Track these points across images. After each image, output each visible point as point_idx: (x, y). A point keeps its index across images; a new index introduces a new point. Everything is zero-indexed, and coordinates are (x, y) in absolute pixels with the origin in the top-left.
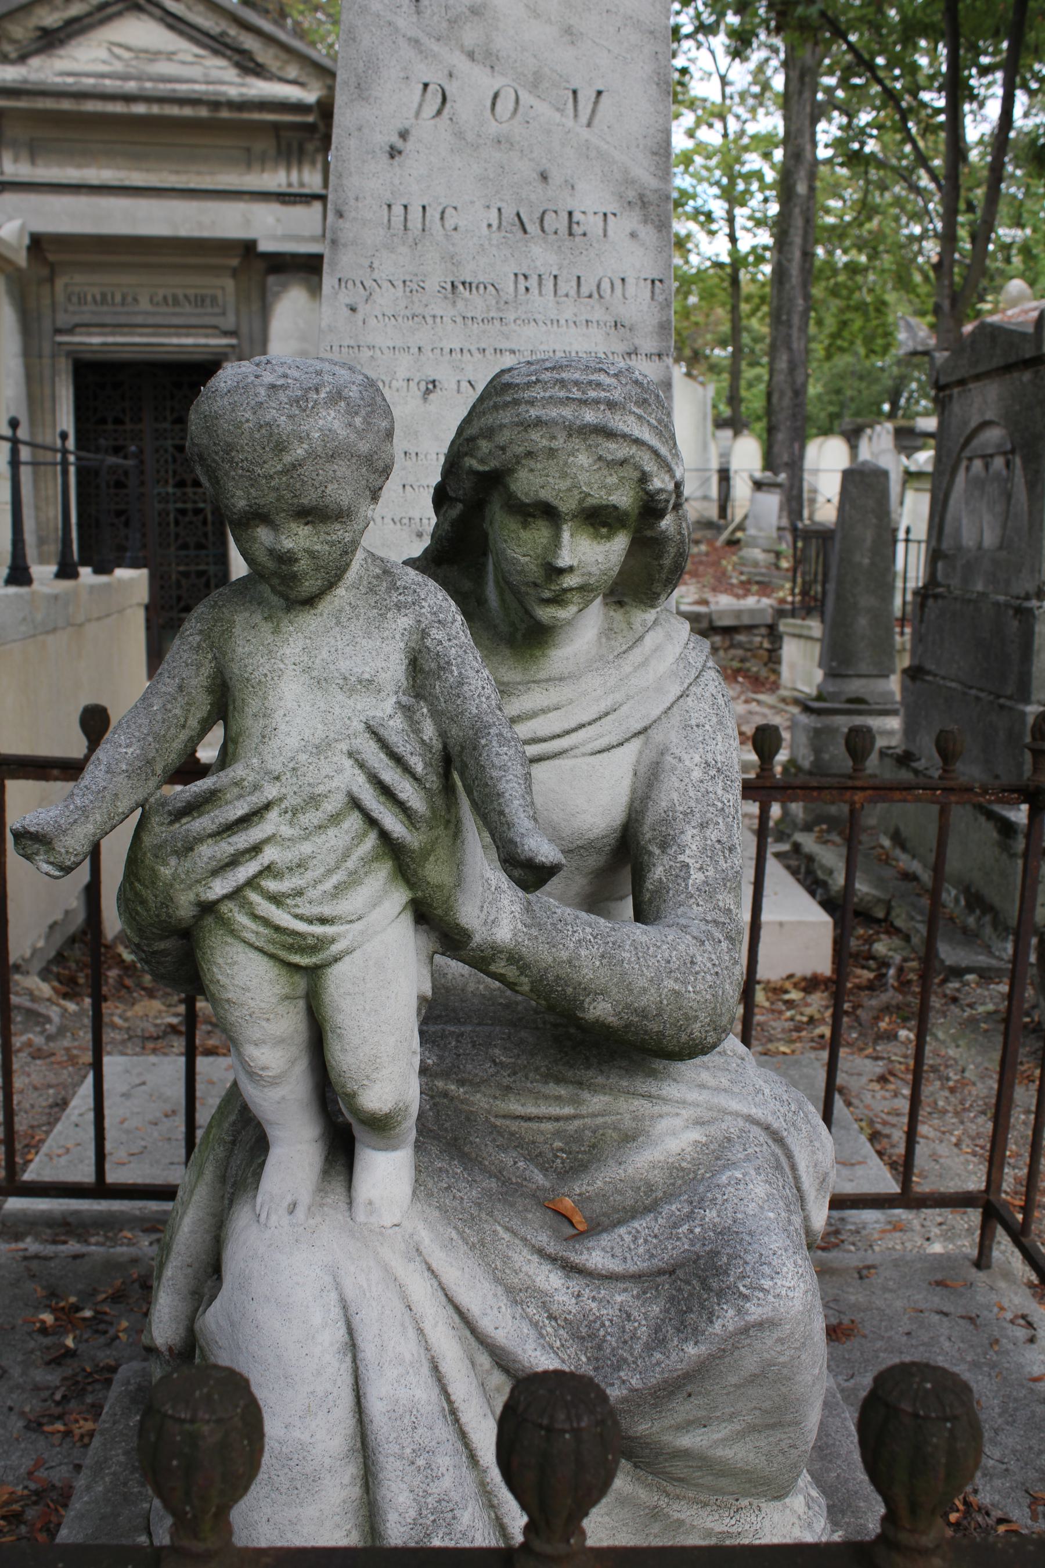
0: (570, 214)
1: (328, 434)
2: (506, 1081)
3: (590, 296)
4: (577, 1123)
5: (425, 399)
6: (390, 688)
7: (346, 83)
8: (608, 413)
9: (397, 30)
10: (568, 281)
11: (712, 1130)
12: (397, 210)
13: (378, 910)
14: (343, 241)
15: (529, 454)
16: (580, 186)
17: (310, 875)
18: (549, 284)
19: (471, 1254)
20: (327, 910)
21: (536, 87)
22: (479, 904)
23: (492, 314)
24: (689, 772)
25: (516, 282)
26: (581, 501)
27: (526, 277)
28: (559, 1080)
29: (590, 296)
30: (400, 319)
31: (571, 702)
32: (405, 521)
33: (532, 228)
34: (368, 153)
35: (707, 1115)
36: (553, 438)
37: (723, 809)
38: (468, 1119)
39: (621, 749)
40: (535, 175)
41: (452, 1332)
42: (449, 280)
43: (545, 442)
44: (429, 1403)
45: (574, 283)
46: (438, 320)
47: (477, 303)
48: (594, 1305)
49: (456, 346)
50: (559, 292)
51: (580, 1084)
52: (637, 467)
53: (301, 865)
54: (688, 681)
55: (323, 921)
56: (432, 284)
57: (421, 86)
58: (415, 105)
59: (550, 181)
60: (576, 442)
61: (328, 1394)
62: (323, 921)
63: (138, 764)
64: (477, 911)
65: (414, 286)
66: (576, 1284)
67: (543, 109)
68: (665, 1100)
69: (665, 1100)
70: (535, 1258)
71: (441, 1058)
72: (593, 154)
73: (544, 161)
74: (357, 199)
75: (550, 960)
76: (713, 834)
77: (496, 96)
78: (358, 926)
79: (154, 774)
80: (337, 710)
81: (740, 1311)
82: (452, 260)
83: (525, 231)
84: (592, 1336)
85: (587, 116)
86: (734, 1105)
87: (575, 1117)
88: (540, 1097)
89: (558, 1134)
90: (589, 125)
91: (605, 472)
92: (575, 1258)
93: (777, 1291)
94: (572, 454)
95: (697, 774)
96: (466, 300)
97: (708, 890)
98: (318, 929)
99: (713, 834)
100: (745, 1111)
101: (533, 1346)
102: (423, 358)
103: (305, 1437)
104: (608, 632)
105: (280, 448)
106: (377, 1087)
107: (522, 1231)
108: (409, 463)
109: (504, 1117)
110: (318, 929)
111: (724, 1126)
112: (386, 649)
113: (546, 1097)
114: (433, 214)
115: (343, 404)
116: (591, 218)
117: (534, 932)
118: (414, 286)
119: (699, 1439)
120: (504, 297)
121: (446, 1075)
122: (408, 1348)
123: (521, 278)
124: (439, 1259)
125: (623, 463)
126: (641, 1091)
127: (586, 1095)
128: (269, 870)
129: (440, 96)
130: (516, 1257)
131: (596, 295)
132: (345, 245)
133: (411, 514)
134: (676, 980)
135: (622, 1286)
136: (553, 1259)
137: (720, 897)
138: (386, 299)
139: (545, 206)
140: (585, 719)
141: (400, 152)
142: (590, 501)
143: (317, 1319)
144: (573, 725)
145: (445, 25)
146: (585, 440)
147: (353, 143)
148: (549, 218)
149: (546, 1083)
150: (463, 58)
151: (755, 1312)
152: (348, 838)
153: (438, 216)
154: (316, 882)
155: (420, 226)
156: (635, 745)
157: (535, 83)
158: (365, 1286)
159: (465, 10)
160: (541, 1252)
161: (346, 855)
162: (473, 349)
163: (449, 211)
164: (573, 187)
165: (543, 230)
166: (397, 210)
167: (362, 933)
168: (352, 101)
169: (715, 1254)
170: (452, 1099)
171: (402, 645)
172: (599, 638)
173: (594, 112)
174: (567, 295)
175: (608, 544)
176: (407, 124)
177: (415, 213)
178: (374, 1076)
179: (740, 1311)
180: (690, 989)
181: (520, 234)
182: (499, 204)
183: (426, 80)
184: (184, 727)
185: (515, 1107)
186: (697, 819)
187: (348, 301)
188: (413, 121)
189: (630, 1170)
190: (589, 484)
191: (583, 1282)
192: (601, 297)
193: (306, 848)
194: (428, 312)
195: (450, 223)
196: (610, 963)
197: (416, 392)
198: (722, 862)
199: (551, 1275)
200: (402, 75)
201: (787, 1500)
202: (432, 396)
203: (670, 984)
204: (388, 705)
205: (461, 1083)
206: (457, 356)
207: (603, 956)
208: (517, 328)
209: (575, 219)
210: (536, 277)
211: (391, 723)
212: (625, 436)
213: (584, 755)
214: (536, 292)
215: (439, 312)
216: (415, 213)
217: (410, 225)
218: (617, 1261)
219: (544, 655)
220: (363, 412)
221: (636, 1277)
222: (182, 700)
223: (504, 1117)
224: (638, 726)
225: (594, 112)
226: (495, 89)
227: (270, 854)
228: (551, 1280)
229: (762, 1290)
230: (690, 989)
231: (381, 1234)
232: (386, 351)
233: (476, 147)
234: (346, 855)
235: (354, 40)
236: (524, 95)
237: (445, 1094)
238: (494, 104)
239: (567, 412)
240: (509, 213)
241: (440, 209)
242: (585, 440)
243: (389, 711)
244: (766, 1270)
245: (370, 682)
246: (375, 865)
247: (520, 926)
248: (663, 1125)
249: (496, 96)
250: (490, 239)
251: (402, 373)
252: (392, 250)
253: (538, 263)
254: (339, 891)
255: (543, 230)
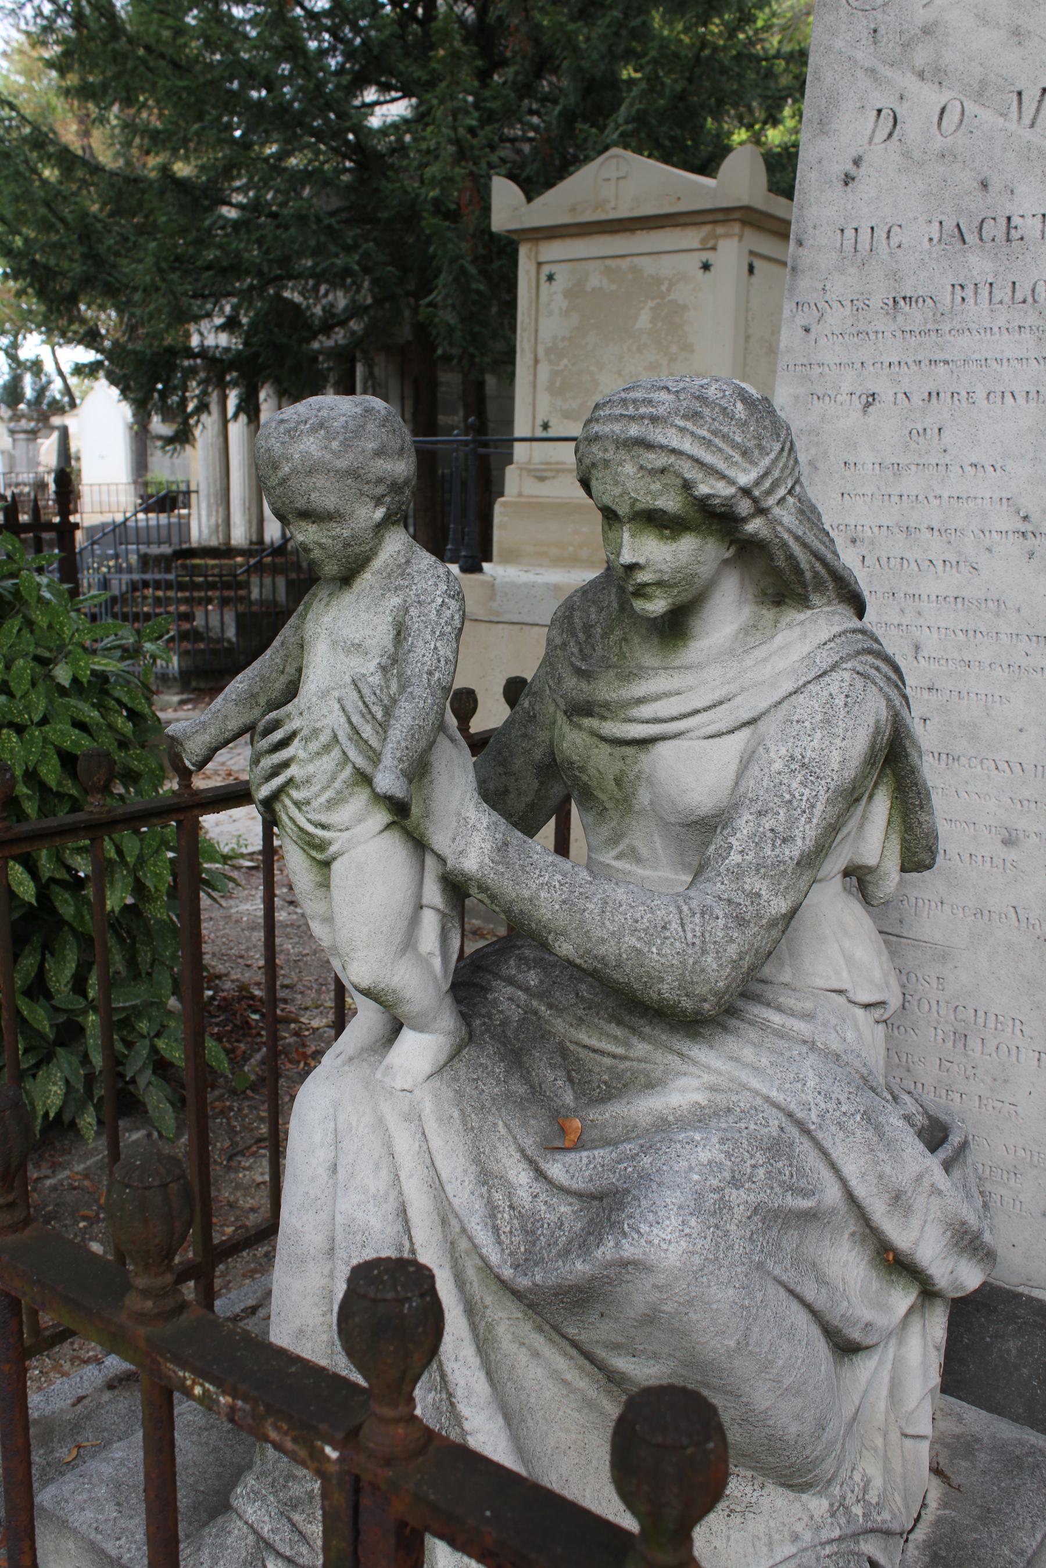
0: (1009, 219)
1: (306, 455)
2: (580, 1013)
3: (1024, 302)
4: (628, 1064)
5: (865, 412)
6: (376, 651)
7: (810, 121)
8: (651, 426)
9: (856, 62)
10: (1003, 288)
11: (719, 1098)
12: (850, 233)
13: (363, 825)
14: (801, 267)
15: (593, 464)
16: (1020, 190)
17: (315, 789)
18: (985, 292)
19: (463, 1133)
20: (323, 818)
21: (981, 95)
22: (451, 835)
23: (929, 326)
24: (771, 763)
25: (953, 293)
26: (632, 505)
27: (962, 287)
28: (620, 1023)
29: (1024, 302)
30: (847, 337)
31: (691, 689)
32: (842, 527)
33: (971, 238)
34: (825, 183)
35: (725, 1084)
36: (606, 450)
37: (790, 802)
38: (542, 1037)
39: (731, 737)
40: (975, 184)
41: (425, 1188)
42: (891, 296)
43: (601, 455)
44: (382, 1232)
45: (1009, 290)
46: (880, 335)
47: (915, 316)
48: (543, 1208)
49: (894, 359)
50: (994, 300)
51: (634, 1030)
52: (678, 475)
53: (308, 781)
54: (804, 679)
55: (323, 827)
56: (876, 302)
57: (875, 113)
58: (869, 132)
59: (990, 188)
60: (623, 454)
61: (317, 1199)
62: (323, 827)
63: (244, 696)
64: (448, 842)
65: (859, 305)
66: (538, 1187)
67: (987, 116)
68: (695, 1063)
69: (695, 1063)
70: (518, 1156)
71: (541, 982)
72: (1034, 155)
73: (985, 168)
74: (815, 227)
75: (514, 895)
76: (768, 823)
77: (943, 111)
78: (346, 835)
79: (257, 704)
80: (339, 666)
81: (617, 1244)
82: (895, 276)
83: (964, 242)
84: (533, 1232)
85: (1031, 117)
86: (755, 1083)
87: (625, 1058)
88: (604, 1034)
89: (611, 1069)
90: (1032, 125)
91: (649, 480)
92: (543, 1166)
93: (651, 1238)
94: (620, 464)
95: (778, 766)
96: (906, 314)
97: (738, 874)
98: (319, 832)
99: (768, 823)
100: (764, 1091)
101: (478, 1220)
102: (865, 373)
103: (299, 1226)
104: (748, 629)
105: (276, 467)
106: (355, 964)
107: (516, 1131)
108: (847, 473)
109: (576, 1043)
110: (319, 832)
111: (735, 1098)
112: (376, 621)
113: (608, 1035)
114: (881, 233)
115: (322, 432)
116: (1029, 220)
117: (501, 868)
118: (859, 305)
119: (632, 1367)
120: (941, 308)
121: (540, 996)
122: (377, 1183)
123: (958, 288)
124: (431, 1126)
125: (663, 471)
126: (675, 1048)
127: (634, 1040)
128: (290, 781)
129: (891, 120)
130: (501, 1149)
131: (1030, 300)
132: (803, 271)
133: (847, 521)
134: (639, 939)
135: (570, 1200)
136: (531, 1162)
137: (748, 880)
138: (836, 318)
139: (984, 215)
140: (699, 705)
141: (853, 179)
142: (639, 506)
143: (318, 1138)
144: (688, 709)
145: (898, 49)
146: (629, 451)
147: (813, 175)
148: (988, 225)
149: (610, 1022)
150: (914, 78)
151: (629, 1250)
152: (333, 764)
153: (885, 235)
154: (317, 796)
155: (868, 247)
156: (745, 733)
157: (980, 92)
158: (354, 1124)
159: (918, 32)
160: (522, 1151)
161: (333, 778)
162: (910, 361)
163: (895, 229)
164: (1012, 191)
165: (981, 239)
166: (850, 233)
167: (349, 840)
168: (814, 136)
169: (627, 1191)
170: (539, 1018)
171: (390, 619)
172: (738, 633)
173: (1038, 110)
174: (1001, 302)
175: (675, 545)
176: (861, 152)
177: (865, 234)
178: (352, 955)
179: (617, 1244)
180: (654, 950)
181: (959, 245)
182: (941, 218)
183: (879, 106)
184: (282, 672)
185: (583, 1036)
186: (758, 806)
187: (804, 323)
188: (866, 147)
189: (632, 1111)
190: (636, 491)
191: (546, 1187)
192: (1035, 301)
193: (310, 768)
194: (871, 329)
195: (894, 241)
196: (570, 910)
197: (858, 404)
198: (768, 851)
199: (523, 1173)
200: (858, 105)
201: (804, 1496)
202: (871, 409)
203: (633, 941)
204: (372, 666)
205: (550, 1006)
206: (895, 369)
207: (564, 902)
208: (951, 339)
209: (1013, 224)
210: (972, 286)
211: (370, 679)
212: (662, 447)
213: (698, 738)
214: (972, 301)
215: (880, 328)
216: (865, 234)
217: (859, 247)
218: (567, 1176)
219: (685, 646)
220: (341, 438)
221: (579, 1195)
222: (282, 653)
223: (576, 1043)
224: (746, 716)
225: (1038, 110)
226: (942, 105)
227: (293, 771)
228: (521, 1177)
229: (639, 1232)
230: (654, 950)
231: (391, 1093)
232: (833, 367)
233: (921, 164)
234: (333, 778)
235: (819, 79)
236: (970, 107)
237: (536, 1013)
238: (941, 118)
239: (617, 428)
240: (950, 225)
241: (886, 229)
242: (629, 451)
243: (372, 669)
244: (651, 1217)
245: (359, 645)
246: (356, 789)
247: (487, 860)
248: (683, 1081)
249: (943, 111)
250: (930, 253)
251: (846, 388)
252: (842, 271)
253: (975, 273)
254: (331, 805)
255: (981, 239)
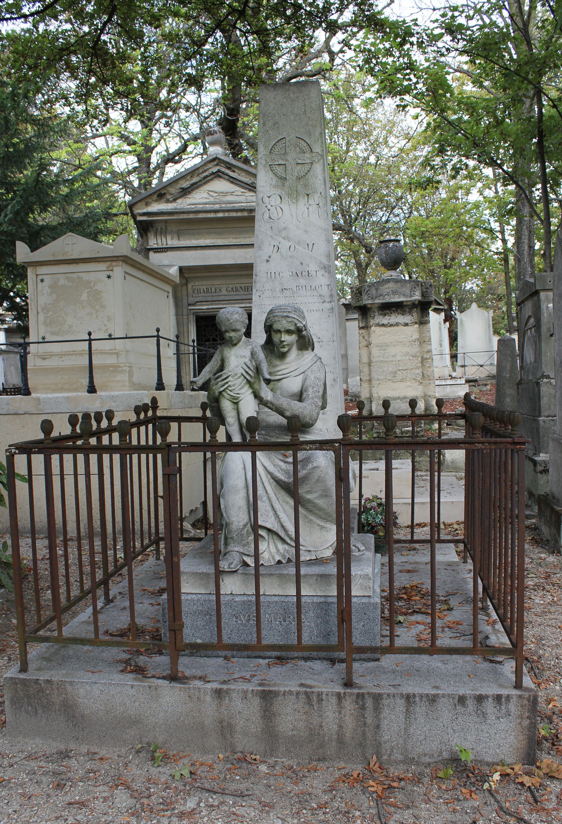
1: (236, 318)
12: (269, 274)
33: (300, 275)
47: (288, 293)
53: (234, 385)
56: (277, 290)
76: (315, 389)
97: (313, 398)
99: (315, 389)
104: (298, 355)
105: (229, 321)
114: (276, 274)
121: (266, 435)
128: (229, 386)
138: (267, 294)
151: (315, 464)
157: (299, 243)
160: (280, 460)
166: (269, 274)
177: (273, 274)
216: (273, 274)
227: (229, 383)
228: (282, 464)
240: (294, 273)
254: (240, 389)
